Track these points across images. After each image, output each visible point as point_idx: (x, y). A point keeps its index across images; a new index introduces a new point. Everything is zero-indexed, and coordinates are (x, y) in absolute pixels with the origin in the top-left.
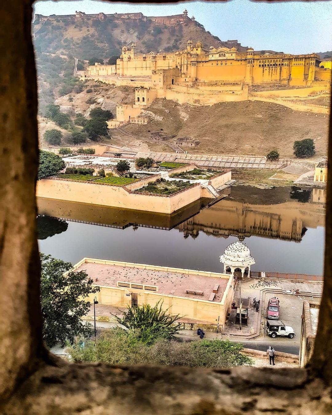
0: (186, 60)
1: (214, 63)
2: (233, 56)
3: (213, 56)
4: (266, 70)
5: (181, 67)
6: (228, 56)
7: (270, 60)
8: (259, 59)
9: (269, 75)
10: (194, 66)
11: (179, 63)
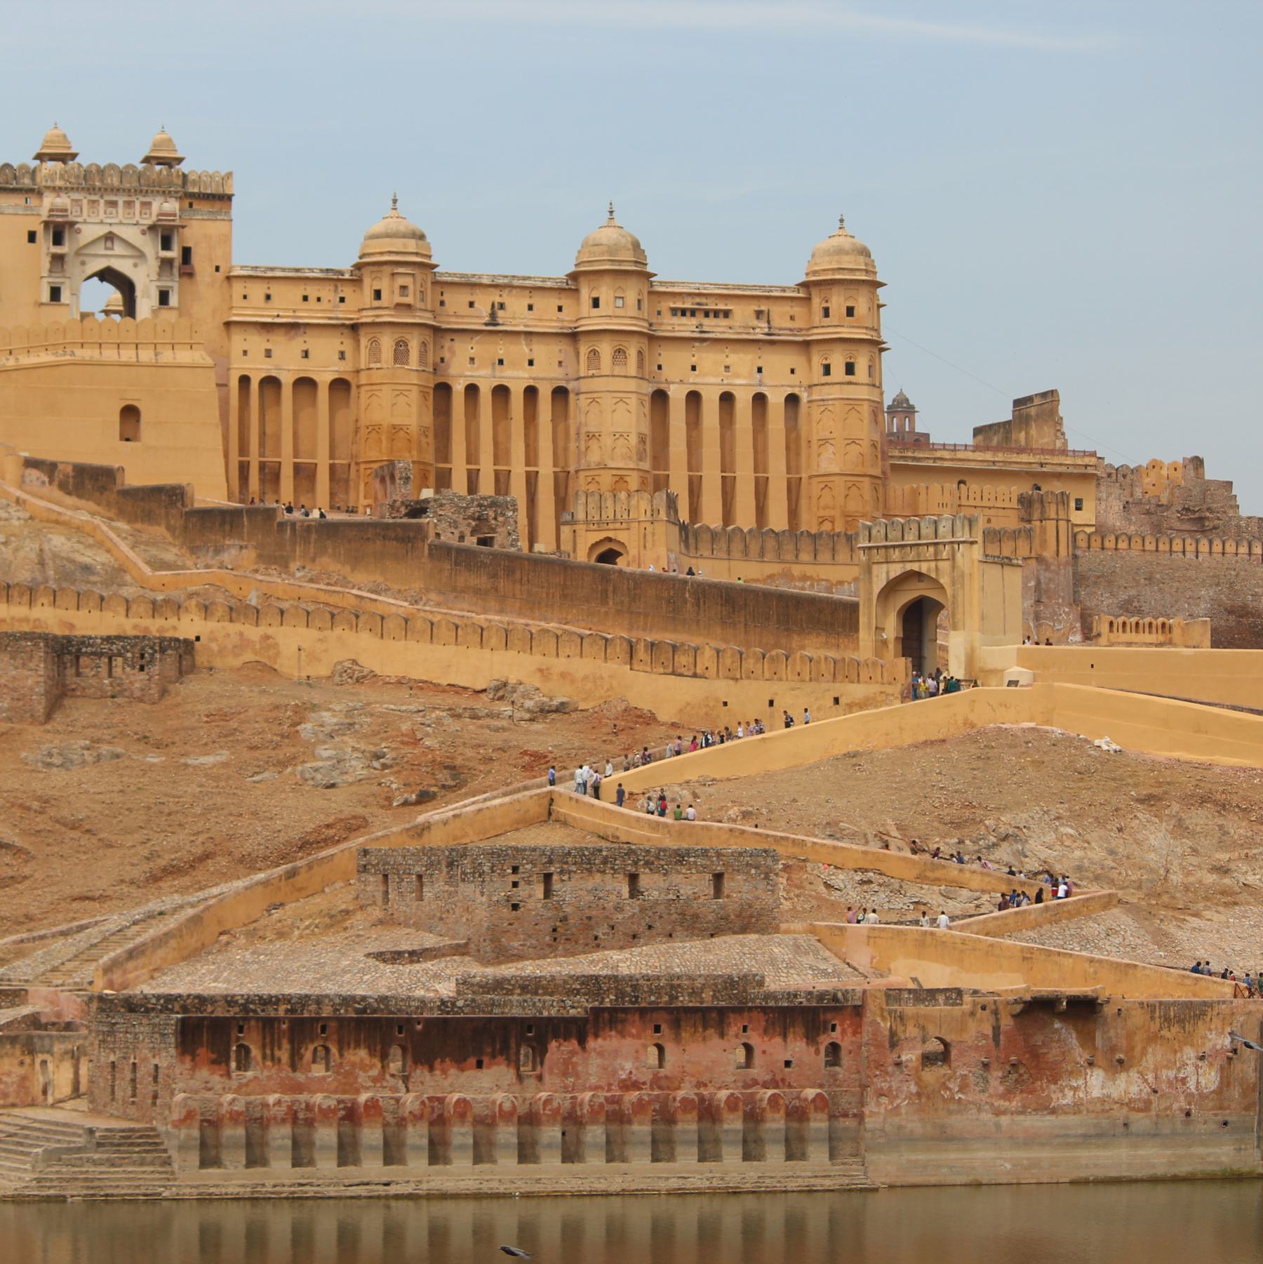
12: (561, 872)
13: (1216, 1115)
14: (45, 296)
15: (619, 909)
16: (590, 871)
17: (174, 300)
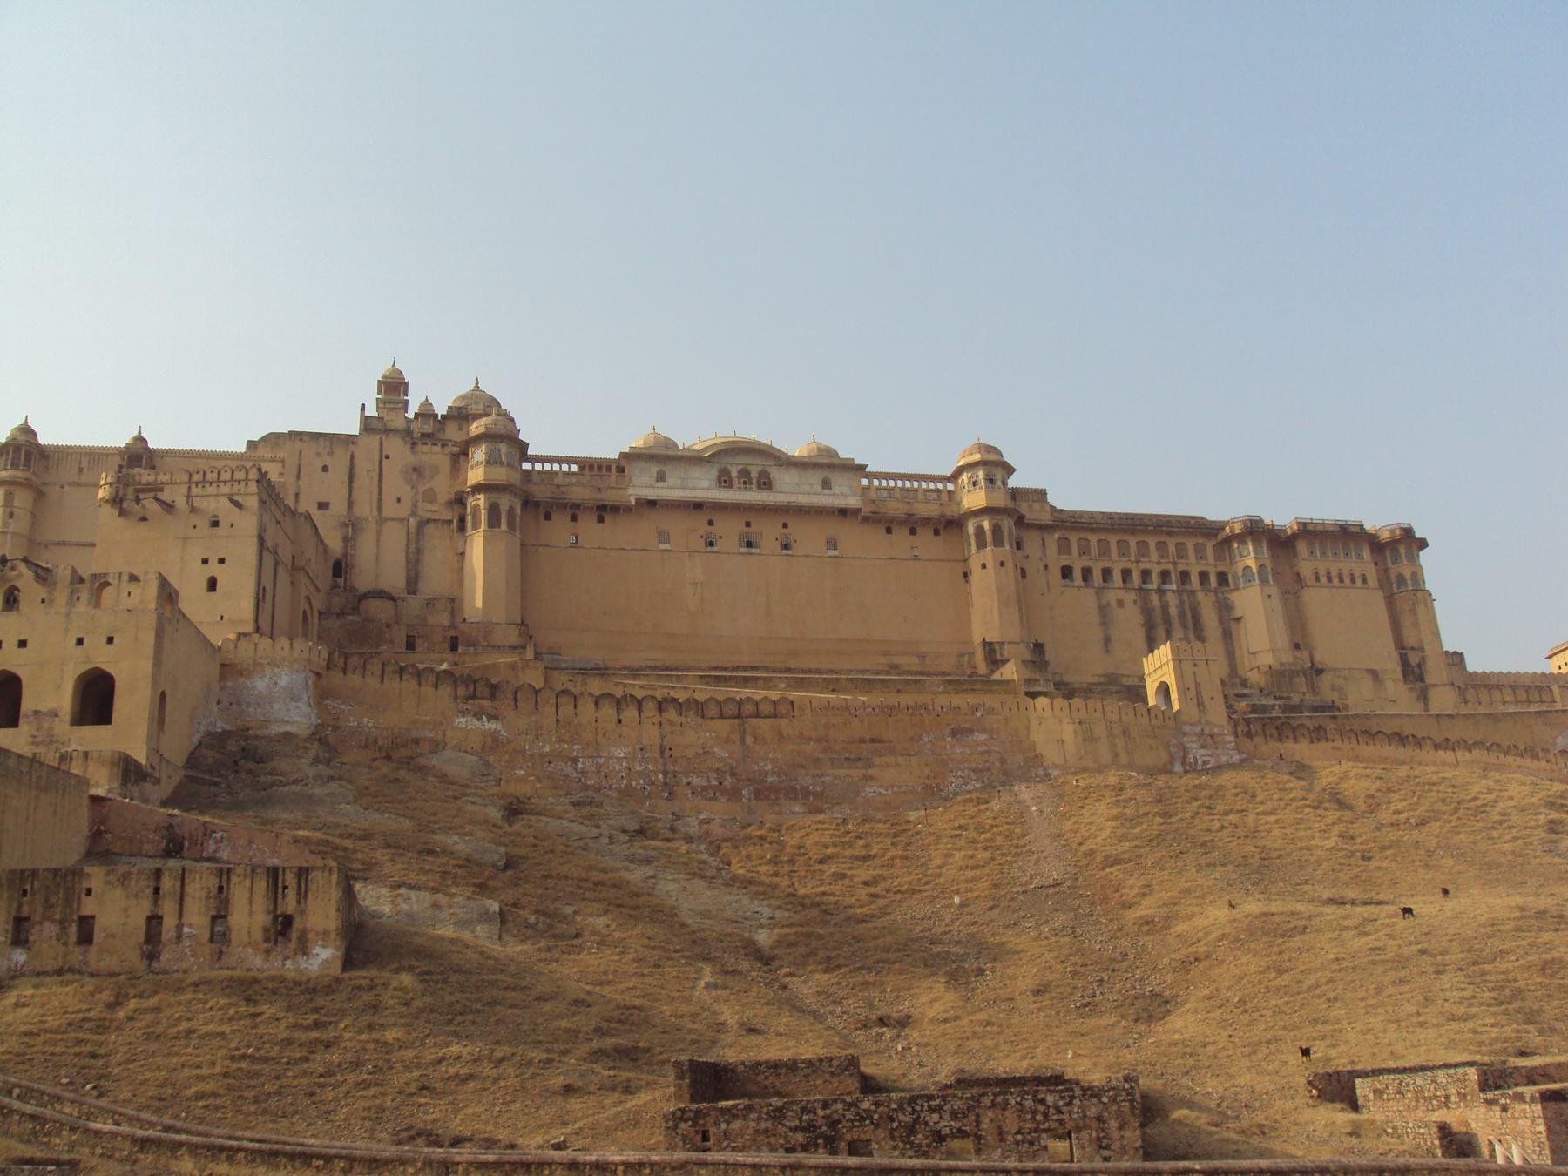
1: (677, 525)
2: (837, 489)
3: (661, 477)
4: (1120, 603)
10: (504, 527)
11: (323, 506)
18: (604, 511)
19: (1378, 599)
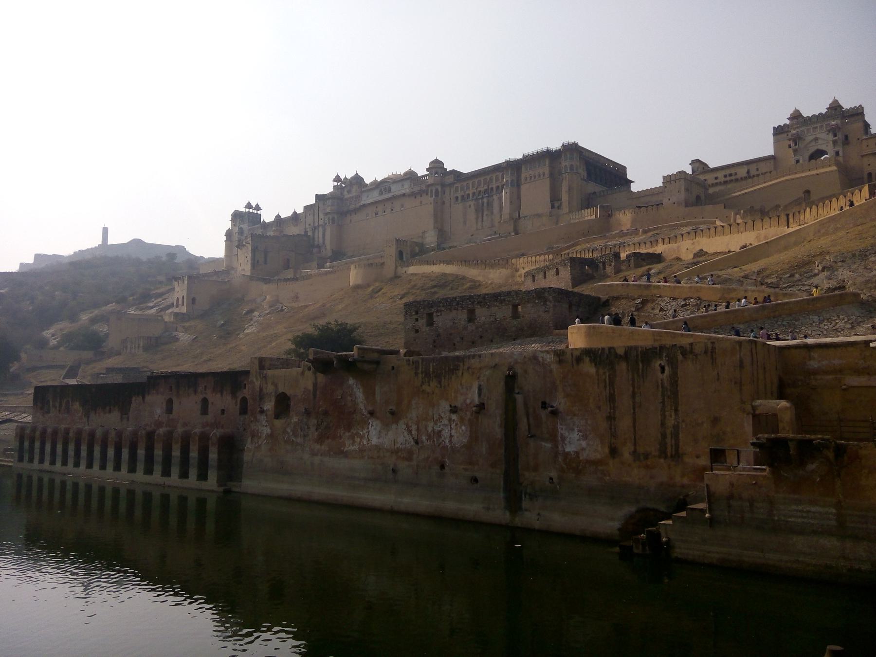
0: (321, 216)
4: (470, 206)
5: (314, 233)
6: (396, 190)
7: (476, 181)
8: (453, 184)
9: (477, 218)
12: (437, 311)
13: (466, 470)
14: (794, 162)
15: (465, 328)
16: (450, 310)
17: (841, 154)
18: (356, 211)
19: (547, 182)
